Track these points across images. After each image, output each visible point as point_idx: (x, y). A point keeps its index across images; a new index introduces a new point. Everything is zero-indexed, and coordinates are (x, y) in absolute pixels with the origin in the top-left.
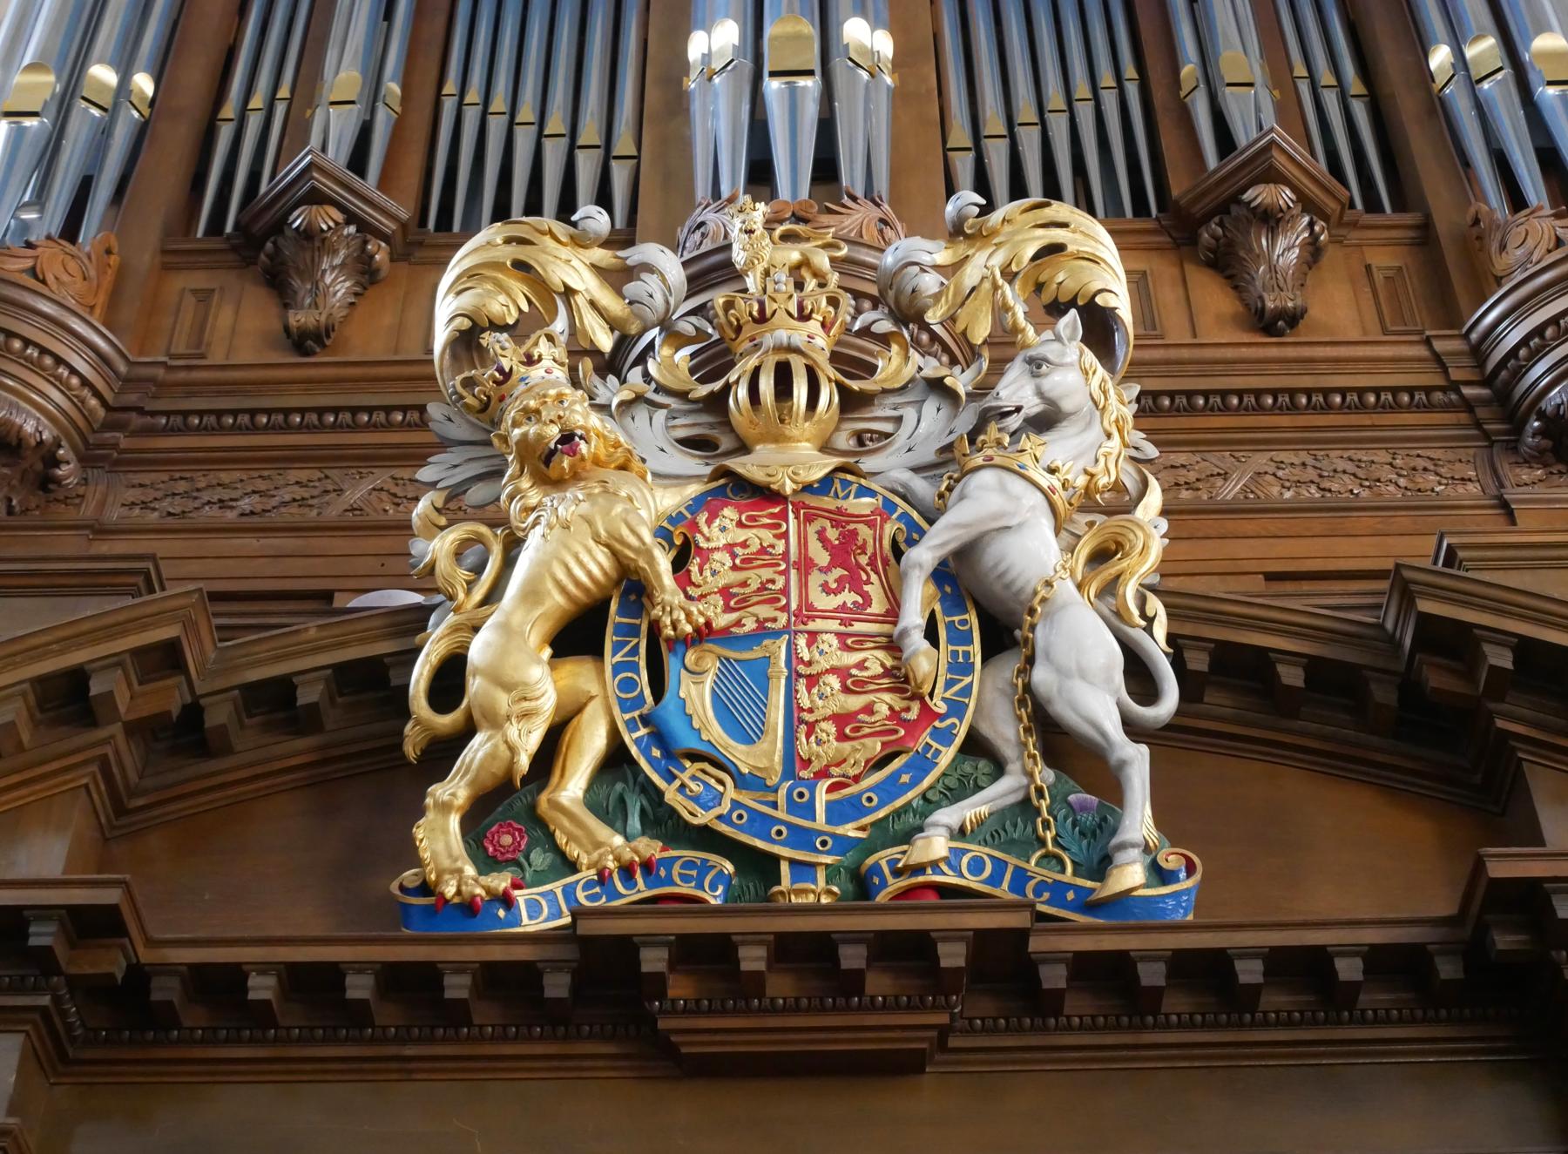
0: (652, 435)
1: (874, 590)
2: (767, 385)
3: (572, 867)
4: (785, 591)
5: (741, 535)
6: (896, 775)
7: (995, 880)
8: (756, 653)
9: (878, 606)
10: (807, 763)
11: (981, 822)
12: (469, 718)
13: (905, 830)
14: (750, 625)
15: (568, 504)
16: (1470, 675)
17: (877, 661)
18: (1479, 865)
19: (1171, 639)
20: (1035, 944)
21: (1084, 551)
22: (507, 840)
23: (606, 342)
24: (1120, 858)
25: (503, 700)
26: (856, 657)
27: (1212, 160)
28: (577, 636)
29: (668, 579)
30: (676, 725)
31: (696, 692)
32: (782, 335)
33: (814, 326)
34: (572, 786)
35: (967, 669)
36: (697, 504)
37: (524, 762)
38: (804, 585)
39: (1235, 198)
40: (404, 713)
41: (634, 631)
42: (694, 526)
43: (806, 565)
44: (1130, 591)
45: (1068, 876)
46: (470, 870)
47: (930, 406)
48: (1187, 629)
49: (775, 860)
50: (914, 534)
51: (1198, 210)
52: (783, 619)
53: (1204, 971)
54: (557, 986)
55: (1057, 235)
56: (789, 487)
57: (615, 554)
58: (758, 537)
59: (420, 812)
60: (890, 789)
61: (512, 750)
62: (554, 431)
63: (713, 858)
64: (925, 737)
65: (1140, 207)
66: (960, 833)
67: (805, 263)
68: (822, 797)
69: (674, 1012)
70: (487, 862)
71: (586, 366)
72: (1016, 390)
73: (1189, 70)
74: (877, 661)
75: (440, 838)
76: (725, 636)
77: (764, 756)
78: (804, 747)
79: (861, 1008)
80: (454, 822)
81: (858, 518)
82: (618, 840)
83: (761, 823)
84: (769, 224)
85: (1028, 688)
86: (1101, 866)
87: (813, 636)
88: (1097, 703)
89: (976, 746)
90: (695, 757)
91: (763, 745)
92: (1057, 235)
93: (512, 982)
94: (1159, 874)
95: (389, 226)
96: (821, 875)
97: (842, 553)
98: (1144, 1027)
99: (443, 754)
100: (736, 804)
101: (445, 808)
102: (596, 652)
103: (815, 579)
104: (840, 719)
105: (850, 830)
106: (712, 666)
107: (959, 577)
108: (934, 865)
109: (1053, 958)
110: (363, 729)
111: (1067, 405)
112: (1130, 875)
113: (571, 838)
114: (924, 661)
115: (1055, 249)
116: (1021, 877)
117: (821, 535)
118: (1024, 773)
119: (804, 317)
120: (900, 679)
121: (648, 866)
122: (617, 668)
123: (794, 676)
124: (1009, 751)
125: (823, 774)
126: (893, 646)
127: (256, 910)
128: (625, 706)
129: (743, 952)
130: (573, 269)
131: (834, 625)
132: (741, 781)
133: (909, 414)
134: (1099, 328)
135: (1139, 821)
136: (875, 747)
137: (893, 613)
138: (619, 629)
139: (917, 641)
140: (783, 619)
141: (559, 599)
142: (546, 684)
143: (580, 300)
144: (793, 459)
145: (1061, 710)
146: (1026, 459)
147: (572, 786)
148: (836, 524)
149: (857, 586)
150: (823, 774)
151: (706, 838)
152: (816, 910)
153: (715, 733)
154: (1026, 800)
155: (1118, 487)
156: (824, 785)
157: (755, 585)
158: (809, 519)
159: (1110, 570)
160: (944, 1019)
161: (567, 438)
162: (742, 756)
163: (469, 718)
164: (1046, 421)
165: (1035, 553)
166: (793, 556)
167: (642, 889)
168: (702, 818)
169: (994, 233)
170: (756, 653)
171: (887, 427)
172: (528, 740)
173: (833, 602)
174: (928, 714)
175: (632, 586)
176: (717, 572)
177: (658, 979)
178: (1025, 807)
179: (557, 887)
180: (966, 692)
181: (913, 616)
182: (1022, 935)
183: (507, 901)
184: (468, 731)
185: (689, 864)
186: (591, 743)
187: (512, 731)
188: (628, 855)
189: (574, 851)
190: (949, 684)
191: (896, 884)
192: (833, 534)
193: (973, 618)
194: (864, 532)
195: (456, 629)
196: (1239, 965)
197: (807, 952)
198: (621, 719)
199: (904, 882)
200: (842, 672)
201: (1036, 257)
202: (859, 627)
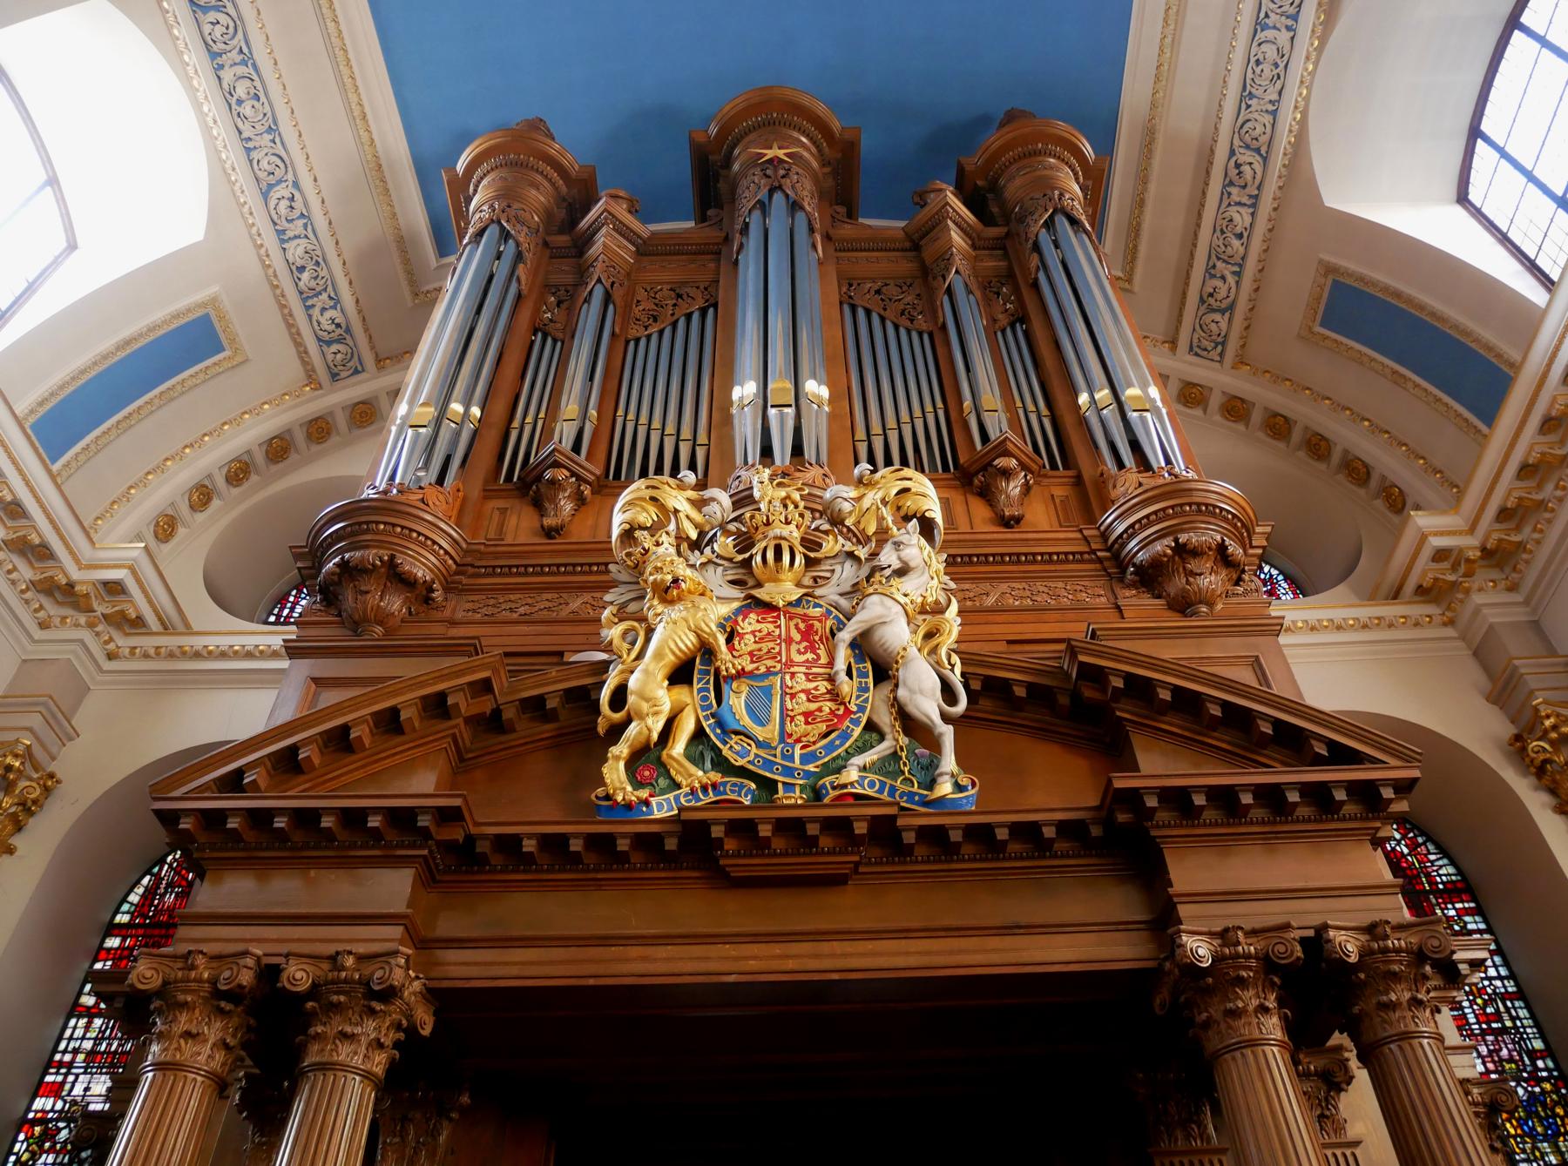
0: (716, 579)
1: (822, 652)
2: (770, 555)
3: (679, 786)
4: (780, 653)
5: (759, 626)
6: (832, 742)
7: (881, 791)
8: (766, 683)
9: (824, 660)
10: (790, 736)
11: (874, 764)
12: (629, 714)
14: (763, 669)
15: (676, 612)
16: (1104, 691)
17: (823, 686)
18: (1110, 781)
19: (963, 674)
20: (900, 822)
21: (921, 633)
22: (647, 773)
23: (694, 535)
24: (940, 780)
25: (645, 706)
26: (813, 685)
27: (979, 446)
28: (680, 675)
29: (723, 647)
30: (728, 718)
31: (737, 702)
32: (778, 532)
33: (792, 527)
34: (678, 747)
35: (866, 690)
36: (738, 612)
37: (655, 736)
38: (788, 650)
39: (990, 464)
40: (598, 712)
41: (707, 673)
42: (736, 622)
43: (789, 641)
44: (943, 652)
46: (629, 788)
47: (848, 565)
48: (971, 670)
49: (776, 782)
50: (841, 626)
51: (972, 470)
52: (779, 666)
53: (980, 834)
54: (671, 844)
55: (907, 484)
56: (781, 604)
57: (698, 636)
58: (767, 627)
59: (606, 760)
60: (830, 748)
61: (649, 730)
62: (669, 578)
63: (746, 782)
64: (847, 723)
65: (946, 468)
66: (864, 769)
67: (788, 497)
68: (798, 752)
69: (727, 856)
70: (638, 784)
71: (684, 546)
72: (888, 557)
73: (967, 404)
74: (823, 686)
75: (615, 773)
76: (750, 675)
77: (769, 733)
78: (789, 728)
79: (817, 854)
80: (622, 765)
81: (814, 618)
82: (700, 773)
83: (768, 764)
84: (771, 480)
85: (895, 698)
86: (931, 784)
87: (793, 675)
88: (928, 705)
89: (871, 726)
90: (737, 733)
91: (770, 727)
92: (907, 484)
93: (649, 843)
94: (959, 787)
95: (591, 478)
96: (798, 790)
97: (807, 634)
98: (952, 861)
99: (616, 731)
100: (757, 756)
101: (617, 758)
102: (690, 683)
103: (794, 647)
104: (807, 715)
105: (811, 768)
106: (745, 689)
107: (862, 646)
108: (852, 784)
109: (908, 828)
110: (578, 720)
111: (912, 564)
112: (945, 788)
113: (678, 772)
114: (846, 686)
115: (906, 490)
116: (893, 790)
117: (796, 626)
118: (894, 739)
119: (788, 523)
120: (834, 695)
121: (714, 786)
122: (700, 690)
123: (784, 694)
124: (887, 729)
126: (831, 679)
127: (525, 808)
128: (704, 709)
129: (760, 827)
130: (678, 500)
131: (803, 669)
132: (759, 744)
133: (838, 568)
134: (927, 527)
135: (949, 762)
136: (823, 727)
137: (831, 664)
138: (700, 672)
139: (843, 677)
140: (779, 666)
141: (672, 658)
142: (665, 698)
143: (681, 515)
144: (783, 590)
145: (911, 709)
146: (893, 590)
147: (678, 747)
150: (798, 741)
151: (742, 772)
152: (795, 806)
153: (747, 722)
154: (895, 753)
155: (937, 602)
156: (799, 746)
158: (791, 618)
159: (934, 642)
160: (856, 858)
161: (676, 581)
162: (759, 732)
163: (629, 714)
164: (902, 572)
165: (898, 634)
167: (712, 797)
168: (740, 762)
169: (877, 483)
170: (766, 683)
171: (828, 575)
172: (657, 725)
173: (802, 658)
174: (848, 712)
175: (707, 651)
176: (747, 644)
177: (720, 840)
178: (895, 756)
179: (671, 796)
180: (866, 700)
181: (841, 665)
182: (893, 818)
183: (647, 803)
184: (628, 721)
185: (735, 785)
186: (687, 727)
187: (650, 721)
188: (705, 780)
189: (679, 779)
190: (858, 697)
191: (833, 794)
192: (802, 626)
193: (869, 665)
194: (817, 625)
195: (622, 672)
196: (997, 831)
197: (791, 827)
198: (701, 714)
199: (837, 793)
201: (898, 493)
202: (815, 670)
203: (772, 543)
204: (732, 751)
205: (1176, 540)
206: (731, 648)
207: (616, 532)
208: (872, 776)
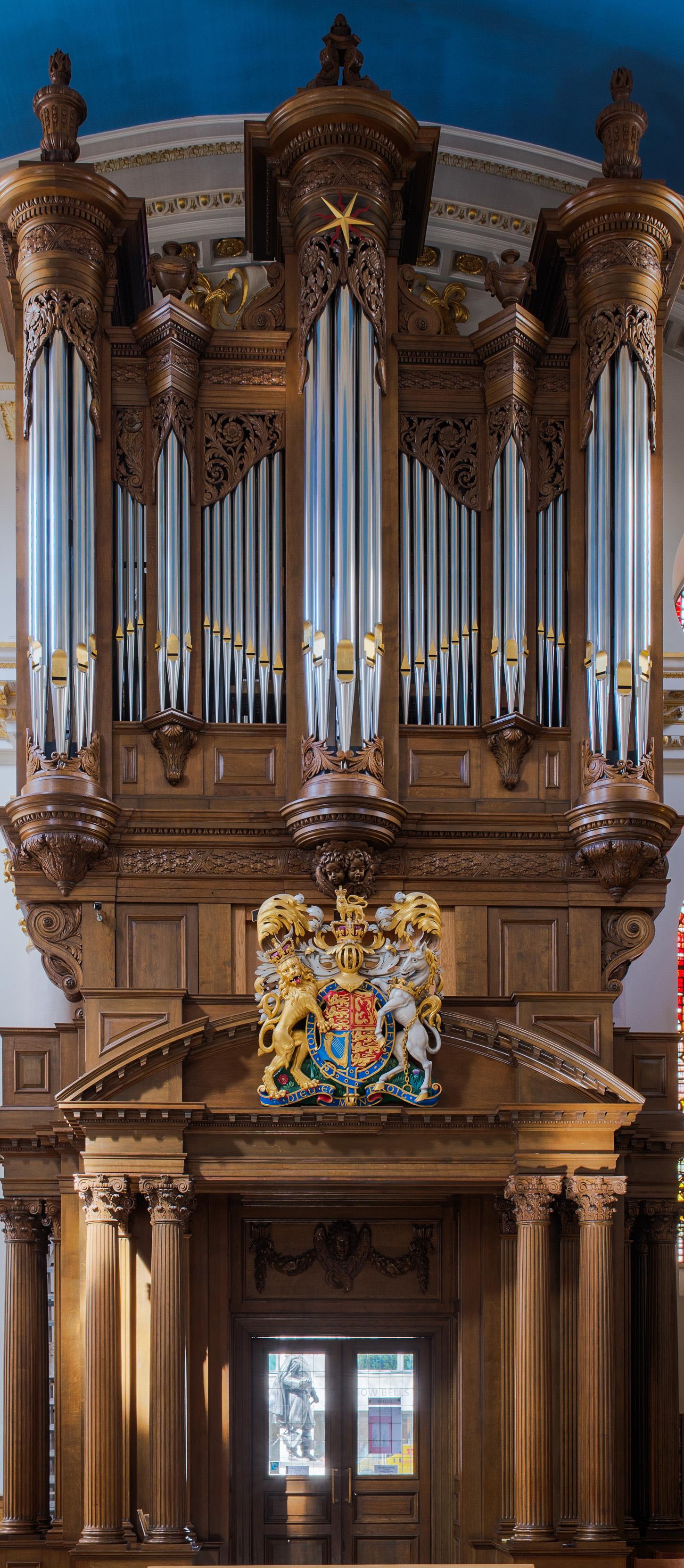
2: (346, 953)
5: (337, 1001)
12: (274, 1050)
13: (375, 1079)
15: (296, 993)
28: (299, 1026)
31: (328, 1042)
41: (312, 1026)
43: (355, 1011)
45: (410, 1093)
58: (343, 1002)
66: (387, 1081)
70: (279, 1086)
77: (343, 1061)
83: (342, 1078)
86: (418, 1092)
87: (355, 1032)
88: (418, 1054)
99: (268, 1058)
103: (357, 1015)
104: (361, 1053)
105: (360, 1080)
116: (400, 1093)
120: (374, 1043)
122: (309, 1036)
124: (399, 1060)
125: (357, 1065)
133: (382, 958)
136: (368, 1060)
138: (309, 1026)
139: (380, 1036)
148: (362, 999)
149: (367, 1018)
151: (330, 1081)
157: (342, 1016)
162: (338, 1062)
163: (274, 1050)
166: (352, 1008)
168: (330, 1076)
171: (376, 961)
178: (401, 1074)
179: (296, 1092)
181: (378, 1029)
184: (274, 1053)
191: (372, 1093)
194: (369, 1003)
200: (362, 1041)
203: (347, 948)
204: (323, 1070)
205: (610, 844)
206: (324, 1015)
207: (261, 936)
208: (391, 1085)
